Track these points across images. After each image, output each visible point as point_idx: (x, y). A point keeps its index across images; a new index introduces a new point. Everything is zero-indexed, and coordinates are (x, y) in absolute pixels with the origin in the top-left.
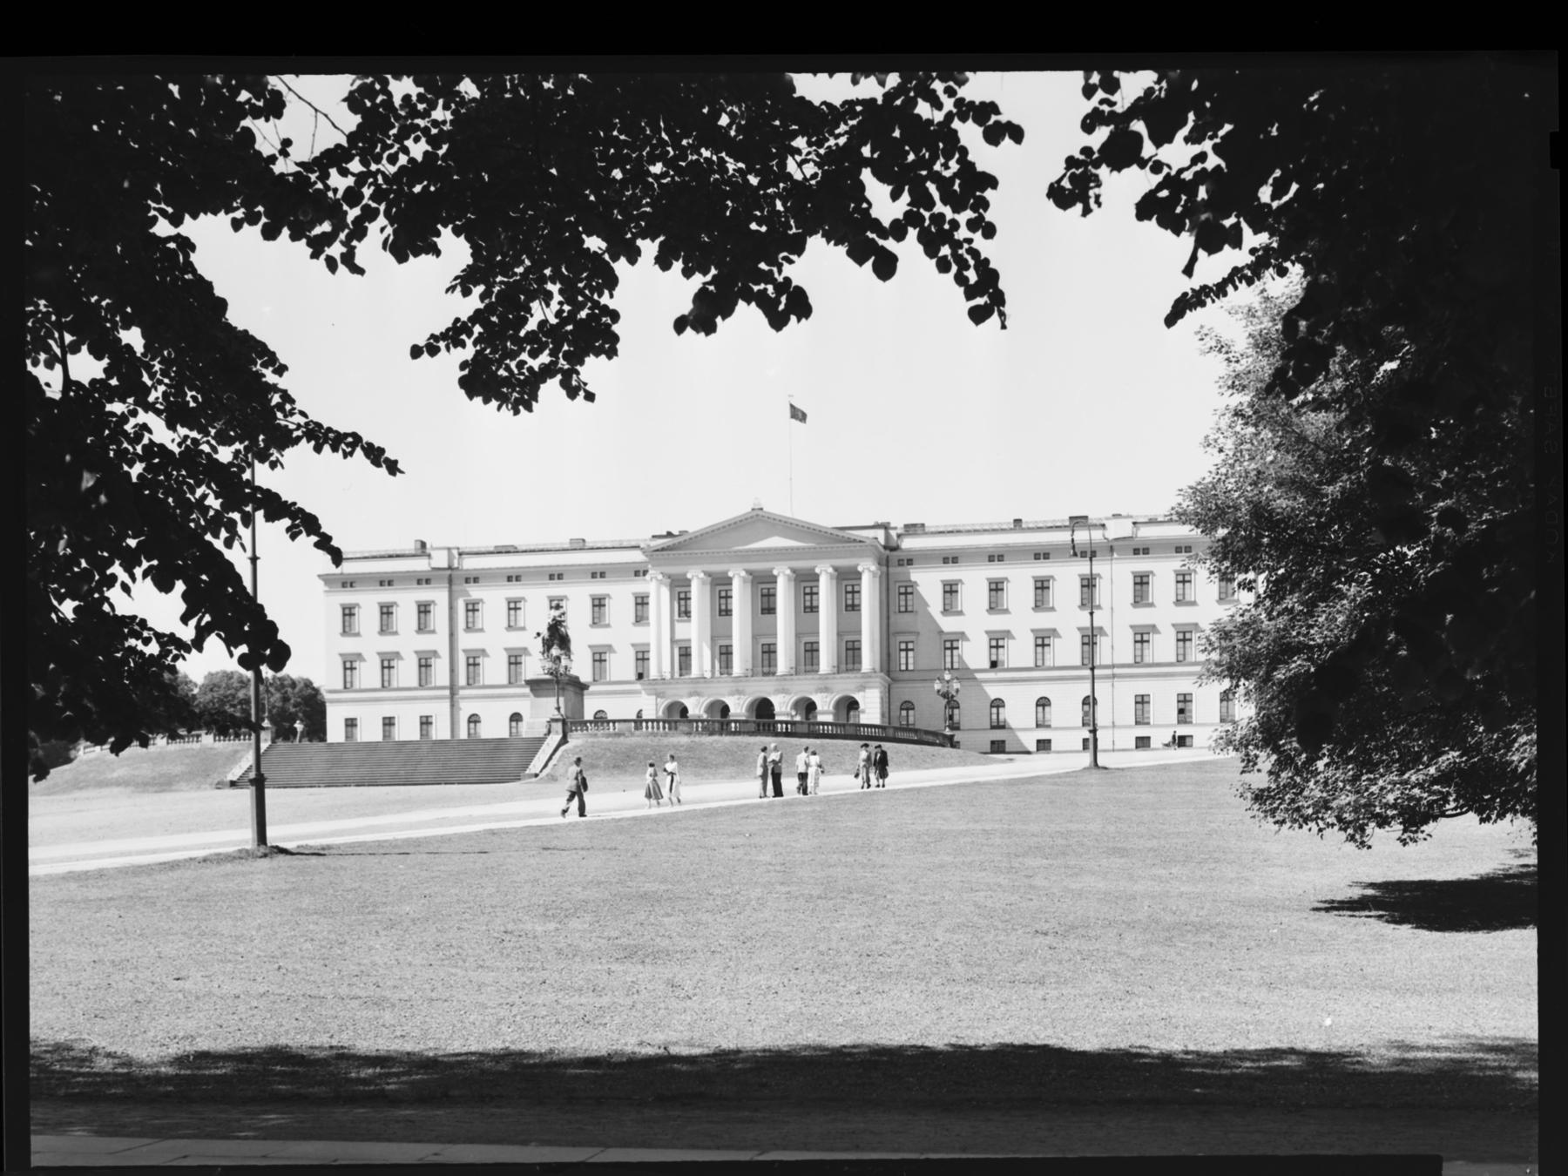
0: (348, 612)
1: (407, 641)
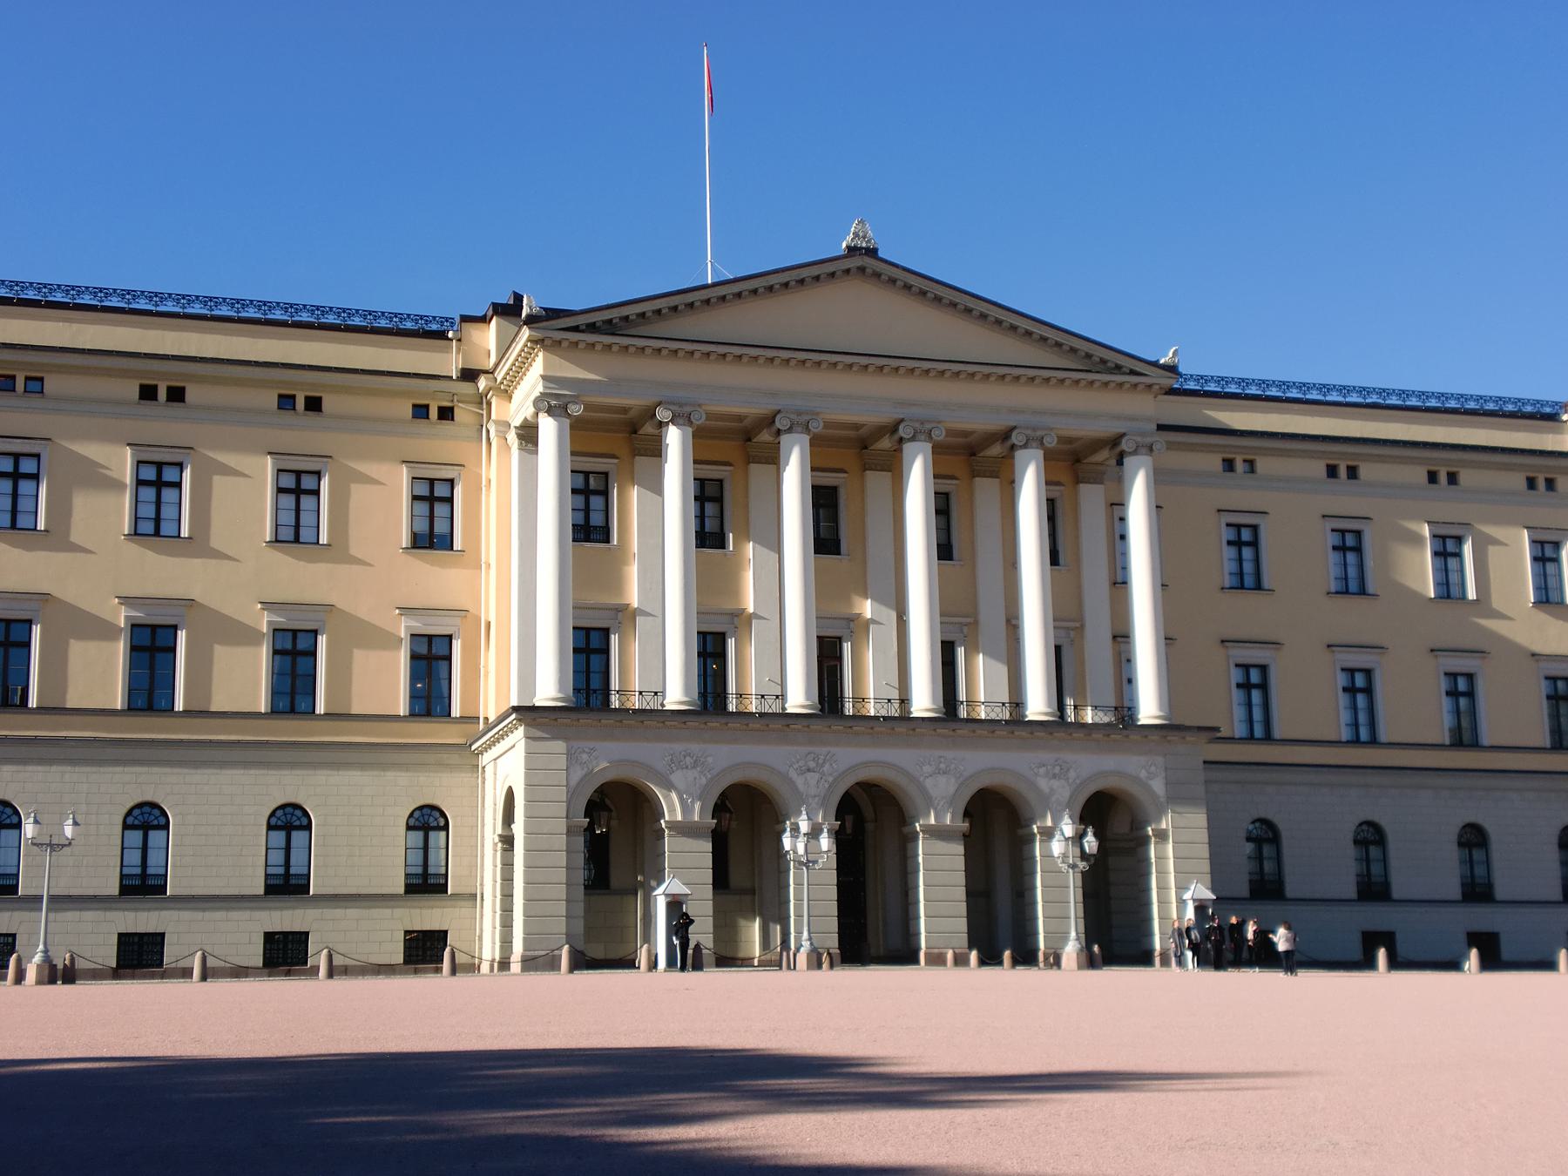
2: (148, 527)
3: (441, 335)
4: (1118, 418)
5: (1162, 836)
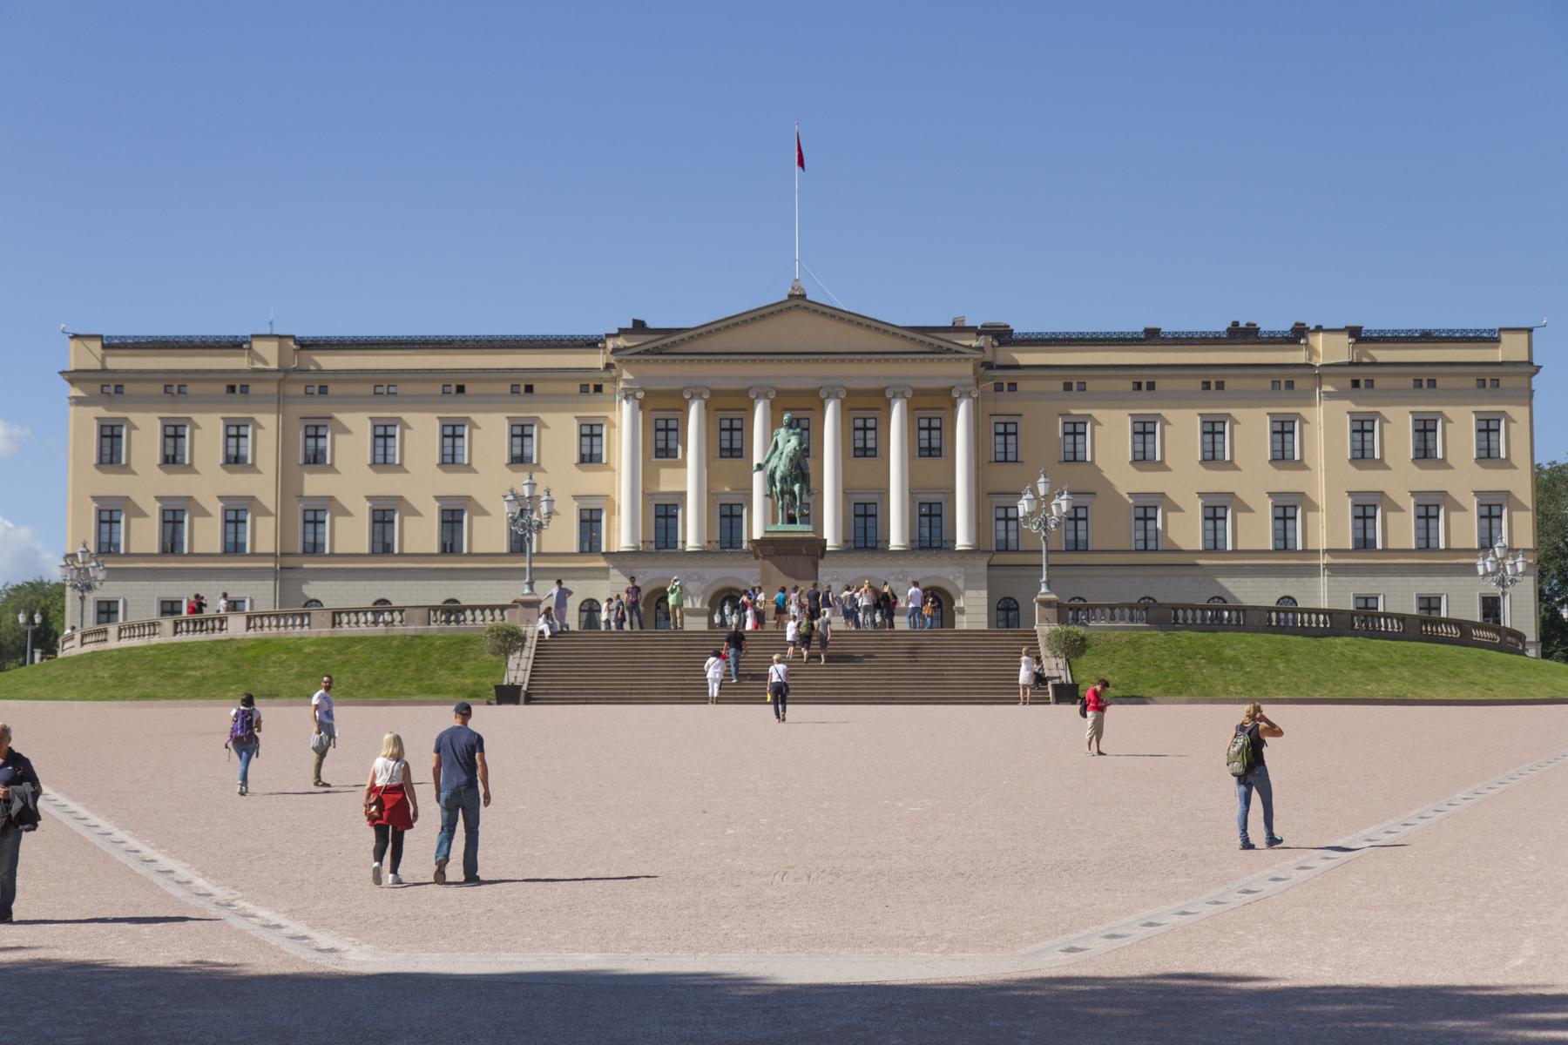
2: (449, 459)
4: (951, 377)
5: (962, 611)
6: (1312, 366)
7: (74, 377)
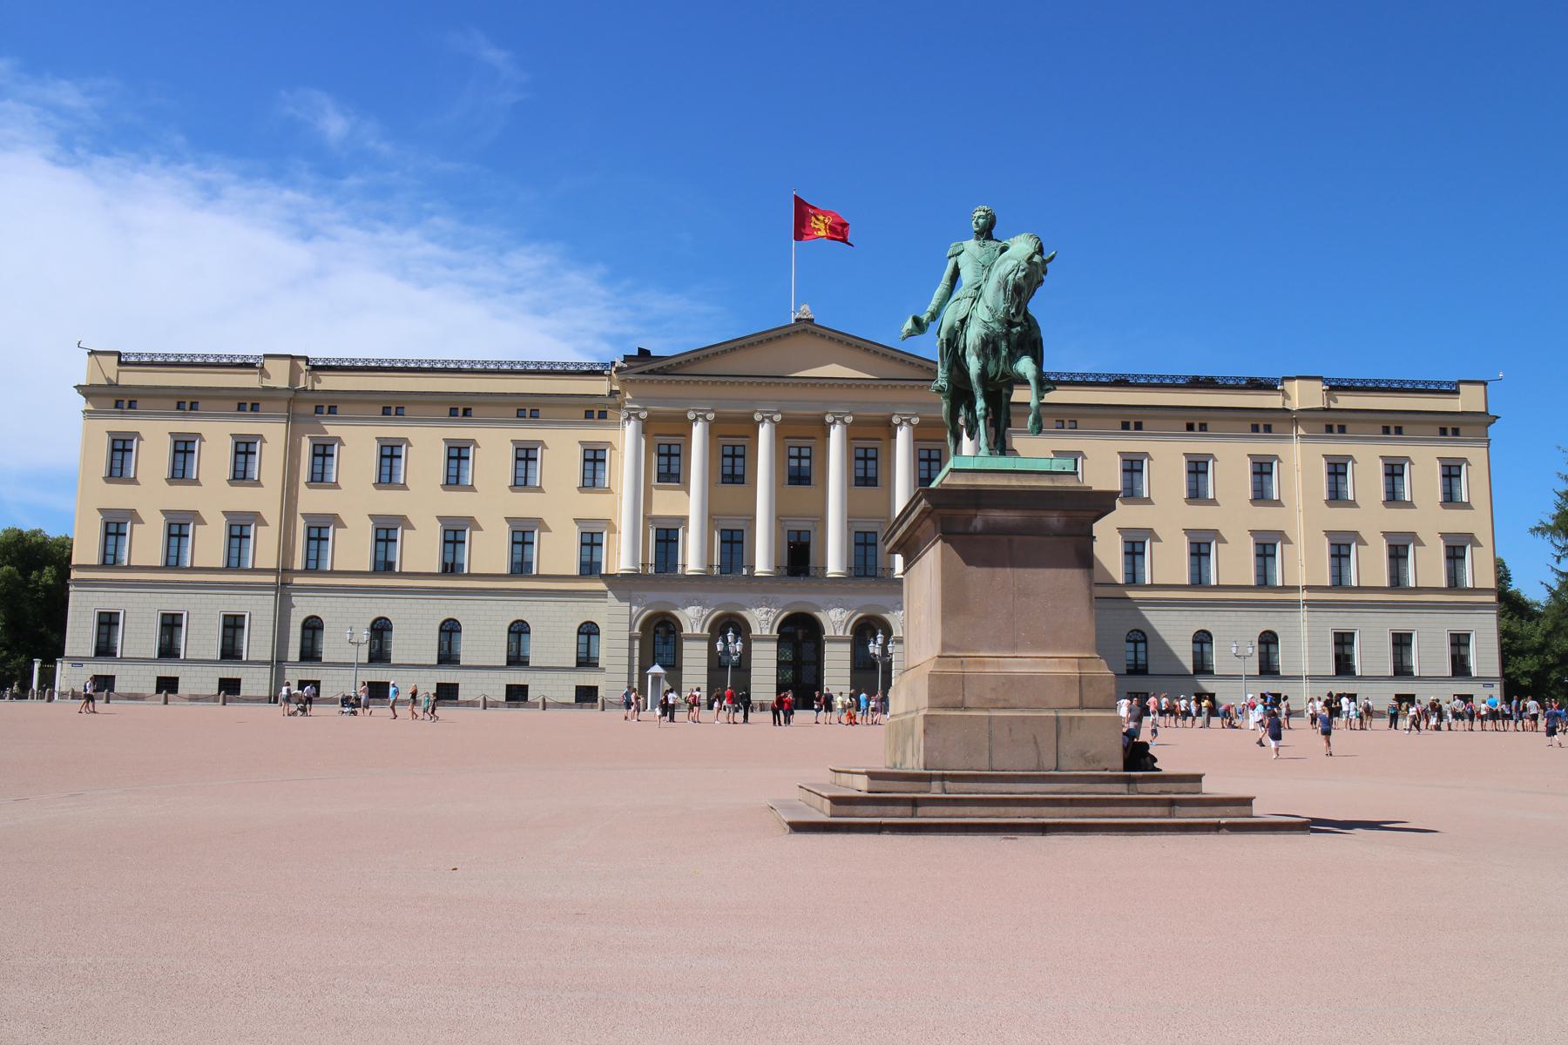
0: (121, 447)
1: (212, 494)
2: (453, 480)
3: (600, 373)
6: (1288, 411)
7: (87, 391)
